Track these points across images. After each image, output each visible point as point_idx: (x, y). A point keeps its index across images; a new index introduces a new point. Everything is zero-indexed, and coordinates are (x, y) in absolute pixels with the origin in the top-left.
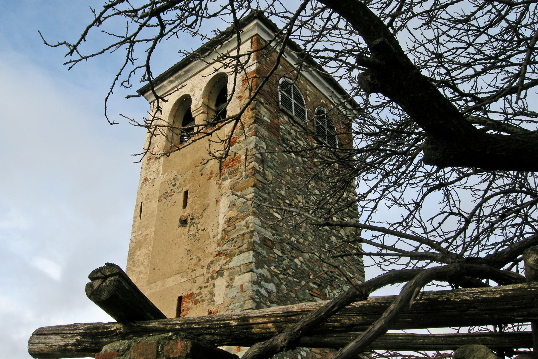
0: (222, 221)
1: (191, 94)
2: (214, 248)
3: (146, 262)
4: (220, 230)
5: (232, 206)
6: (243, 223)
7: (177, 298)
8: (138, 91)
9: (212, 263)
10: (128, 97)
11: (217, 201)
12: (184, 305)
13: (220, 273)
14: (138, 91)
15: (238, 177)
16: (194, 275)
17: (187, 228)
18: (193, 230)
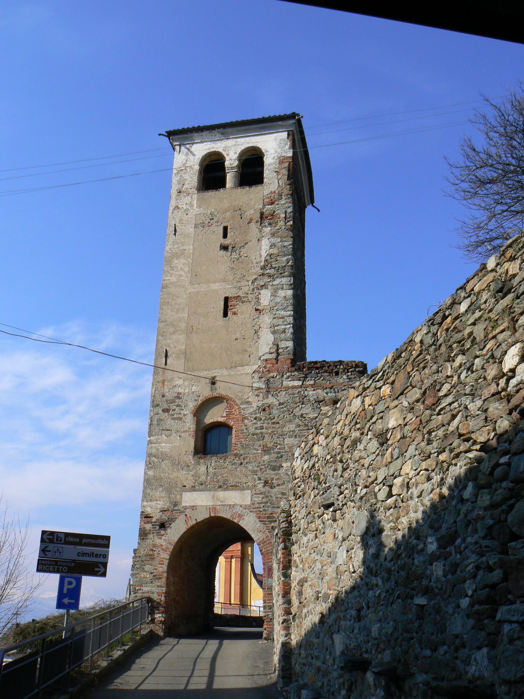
0: (264, 254)
1: (224, 154)
3: (187, 269)
4: (263, 259)
7: (223, 297)
8: (166, 132)
9: (255, 279)
10: (160, 135)
11: (258, 240)
14: (166, 132)
15: (277, 228)
16: (239, 284)
17: (229, 254)
18: (235, 256)
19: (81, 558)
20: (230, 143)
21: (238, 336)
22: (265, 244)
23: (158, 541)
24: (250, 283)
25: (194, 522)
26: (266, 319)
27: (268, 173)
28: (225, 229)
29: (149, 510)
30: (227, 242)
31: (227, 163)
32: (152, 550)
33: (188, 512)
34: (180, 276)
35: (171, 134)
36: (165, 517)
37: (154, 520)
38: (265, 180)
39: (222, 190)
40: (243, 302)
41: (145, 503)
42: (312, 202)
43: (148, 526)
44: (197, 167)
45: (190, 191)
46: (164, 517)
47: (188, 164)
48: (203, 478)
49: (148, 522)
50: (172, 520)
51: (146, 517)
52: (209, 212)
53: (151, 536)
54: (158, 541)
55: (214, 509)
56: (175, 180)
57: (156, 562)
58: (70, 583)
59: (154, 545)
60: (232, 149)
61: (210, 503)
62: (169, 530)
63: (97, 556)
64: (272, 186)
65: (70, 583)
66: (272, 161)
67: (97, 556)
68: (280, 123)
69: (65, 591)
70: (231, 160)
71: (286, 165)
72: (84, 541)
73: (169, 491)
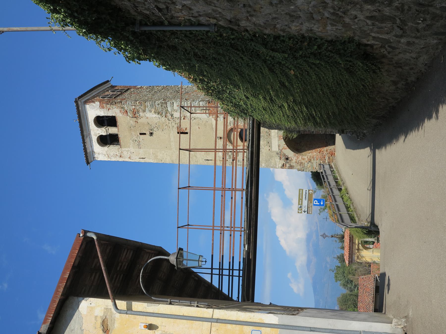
2: (163, 119)
3: (163, 152)
5: (150, 111)
6: (157, 106)
9: (168, 119)
13: (172, 115)
16: (171, 127)
17: (154, 132)
19: (307, 199)
20: (92, 133)
21: (197, 128)
22: (148, 114)
24: (170, 122)
25: (286, 146)
28: (141, 134)
29: (280, 165)
30: (148, 133)
33: (281, 148)
35: (88, 163)
36: (283, 158)
38: (114, 115)
39: (119, 136)
41: (277, 167)
42: (108, 81)
43: (288, 165)
48: (265, 142)
49: (286, 165)
50: (285, 155)
51: (283, 166)
52: (132, 142)
53: (292, 164)
54: (294, 161)
56: (113, 159)
57: (303, 161)
58: (316, 202)
59: (296, 162)
61: (277, 139)
64: (117, 112)
65: (316, 202)
66: (102, 112)
68: (80, 109)
70: (102, 131)
73: (271, 157)
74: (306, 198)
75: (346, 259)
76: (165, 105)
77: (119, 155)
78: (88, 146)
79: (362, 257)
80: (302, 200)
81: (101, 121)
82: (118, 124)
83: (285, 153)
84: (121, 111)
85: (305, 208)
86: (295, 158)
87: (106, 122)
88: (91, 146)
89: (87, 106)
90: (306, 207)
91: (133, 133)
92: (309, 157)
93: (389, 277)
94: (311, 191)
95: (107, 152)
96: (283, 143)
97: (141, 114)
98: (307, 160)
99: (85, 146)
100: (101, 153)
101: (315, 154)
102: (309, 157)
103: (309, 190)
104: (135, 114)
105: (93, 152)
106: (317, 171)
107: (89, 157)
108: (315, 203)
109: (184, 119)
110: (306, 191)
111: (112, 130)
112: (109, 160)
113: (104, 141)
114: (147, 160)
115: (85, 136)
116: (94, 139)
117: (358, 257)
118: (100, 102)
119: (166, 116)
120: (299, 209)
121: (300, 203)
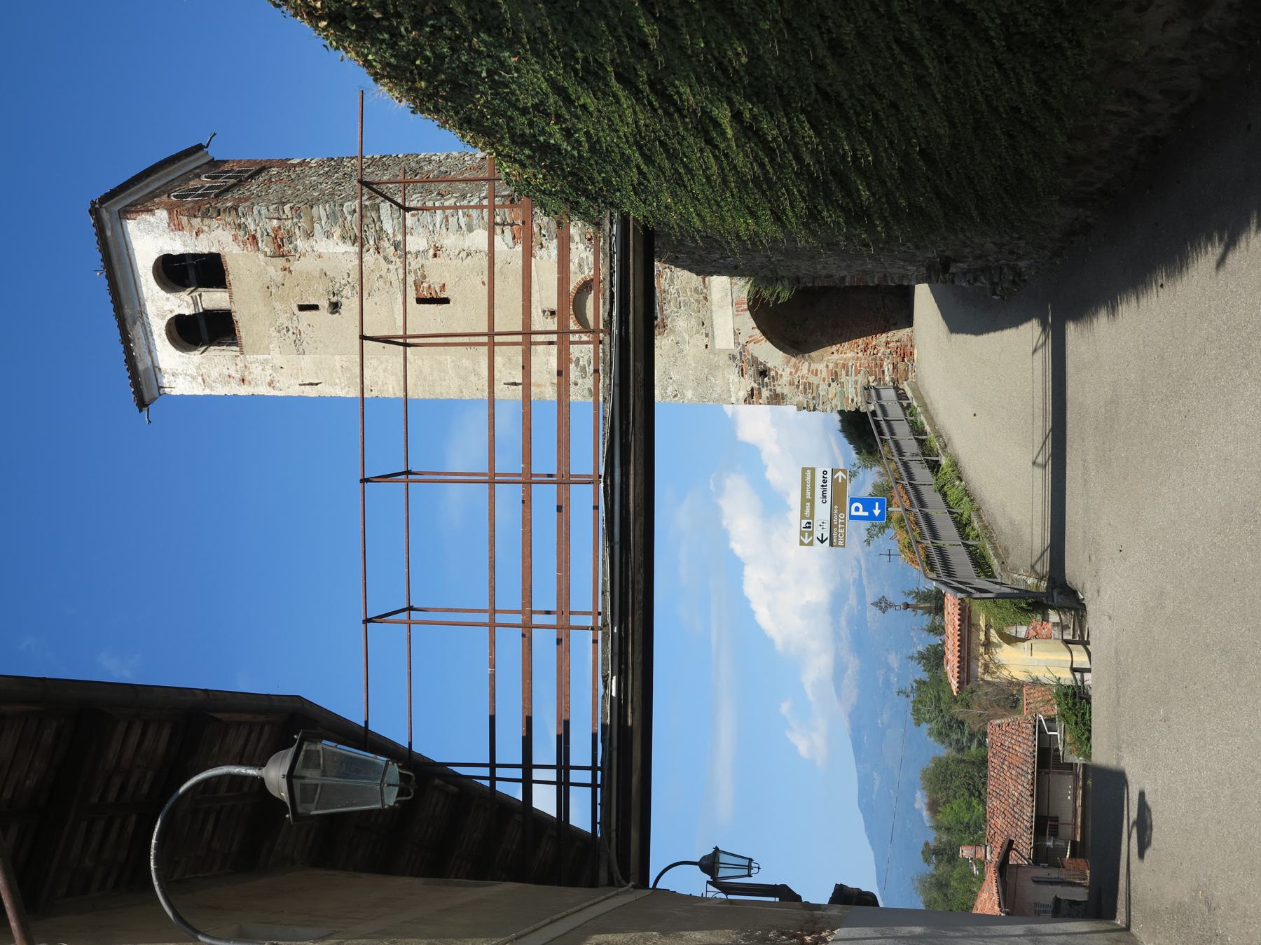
1: (170, 316)
5: (329, 235)
6: (349, 217)
9: (385, 258)
12: (426, 294)
15: (297, 230)
17: (344, 301)
20: (151, 309)
23: (785, 379)
24: (392, 267)
25: (757, 331)
26: (450, 241)
27: (202, 246)
28: (302, 308)
29: (743, 394)
30: (324, 304)
31: (188, 311)
32: (798, 387)
33: (742, 341)
34: (385, 370)
35: (142, 404)
37: (756, 386)
38: (214, 250)
39: (236, 317)
40: (424, 277)
42: (199, 147)
43: (765, 393)
44: (195, 357)
45: (241, 365)
46: (750, 372)
47: (193, 371)
48: (693, 322)
49: (760, 393)
50: (755, 361)
51: (751, 397)
52: (275, 334)
53: (779, 390)
54: (785, 379)
55: (736, 304)
56: (220, 390)
57: (812, 379)
58: (857, 509)
59: (791, 383)
60: (162, 305)
61: (730, 311)
62: (769, 365)
63: (825, 481)
64: (223, 239)
65: (857, 509)
67: (825, 481)
68: (109, 233)
69: (866, 514)
70: (182, 303)
71: (184, 219)
72: (808, 497)
73: (713, 368)
74: (824, 497)
75: (950, 675)
76: (374, 215)
77: (238, 376)
78: (139, 350)
79: (999, 666)
80: (812, 502)
81: (175, 272)
82: (231, 278)
83: (756, 355)
84: (235, 238)
85: (821, 529)
86: (788, 370)
87: (192, 273)
88: (150, 352)
89: (131, 225)
90: (827, 526)
91: (278, 305)
92: (831, 366)
93: (1142, 795)
94: (840, 474)
95: (198, 368)
96: (747, 322)
97: (299, 243)
98: (824, 374)
99: (128, 351)
100: (183, 372)
101: (850, 355)
102: (831, 366)
103: (834, 472)
104: (281, 247)
105: (156, 369)
106: (858, 410)
107: (145, 390)
108: (854, 513)
109: (435, 256)
110: (825, 472)
111: (213, 299)
112: (208, 392)
113: (188, 333)
114: (325, 390)
115: (129, 320)
116: (158, 327)
117: (986, 666)
118: (170, 213)
119: (378, 250)
120: (802, 534)
121: (808, 511)
